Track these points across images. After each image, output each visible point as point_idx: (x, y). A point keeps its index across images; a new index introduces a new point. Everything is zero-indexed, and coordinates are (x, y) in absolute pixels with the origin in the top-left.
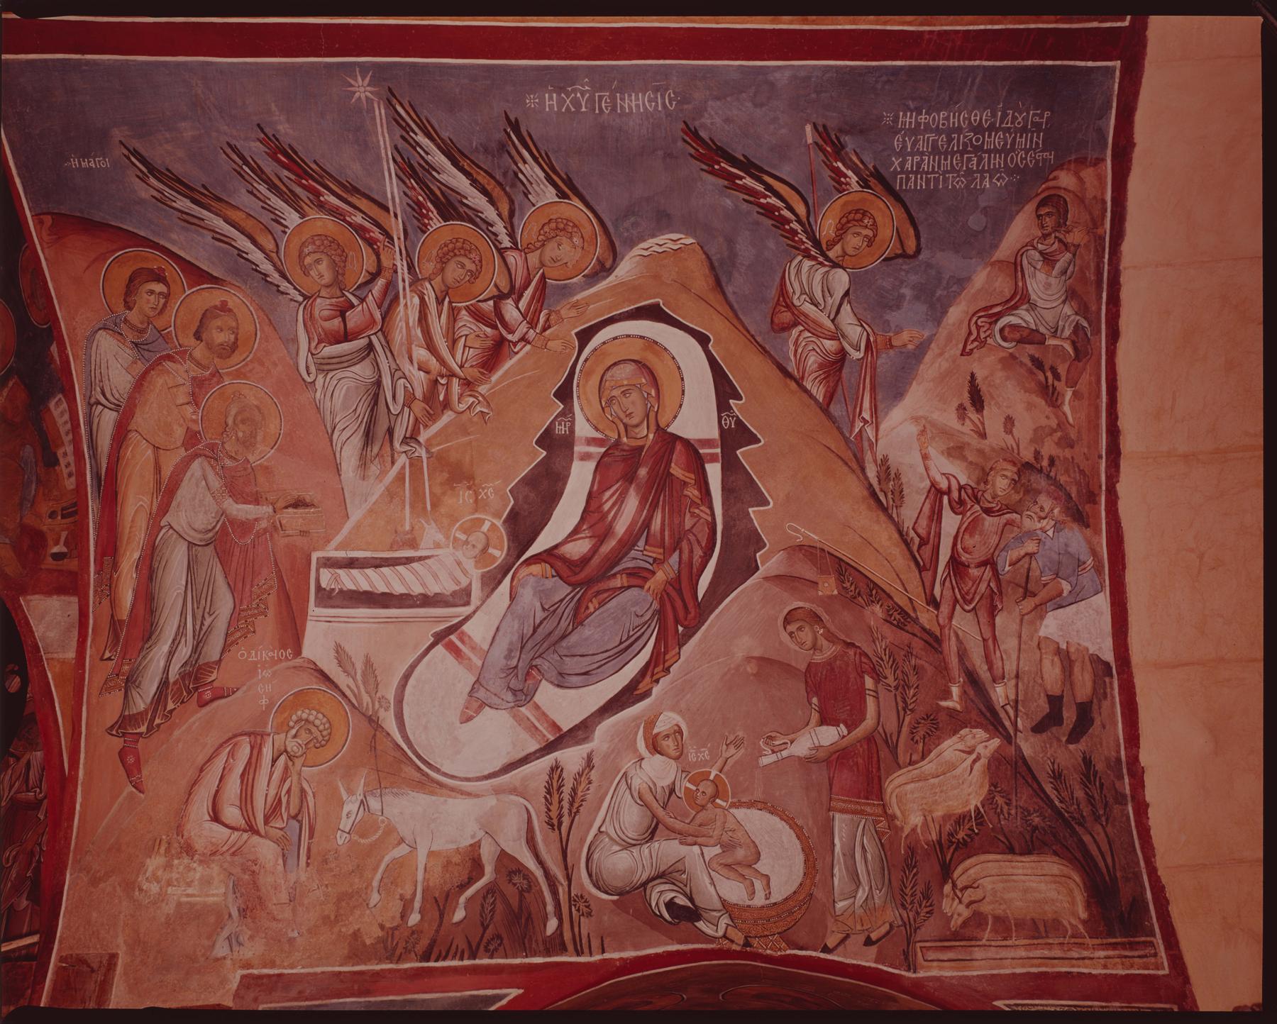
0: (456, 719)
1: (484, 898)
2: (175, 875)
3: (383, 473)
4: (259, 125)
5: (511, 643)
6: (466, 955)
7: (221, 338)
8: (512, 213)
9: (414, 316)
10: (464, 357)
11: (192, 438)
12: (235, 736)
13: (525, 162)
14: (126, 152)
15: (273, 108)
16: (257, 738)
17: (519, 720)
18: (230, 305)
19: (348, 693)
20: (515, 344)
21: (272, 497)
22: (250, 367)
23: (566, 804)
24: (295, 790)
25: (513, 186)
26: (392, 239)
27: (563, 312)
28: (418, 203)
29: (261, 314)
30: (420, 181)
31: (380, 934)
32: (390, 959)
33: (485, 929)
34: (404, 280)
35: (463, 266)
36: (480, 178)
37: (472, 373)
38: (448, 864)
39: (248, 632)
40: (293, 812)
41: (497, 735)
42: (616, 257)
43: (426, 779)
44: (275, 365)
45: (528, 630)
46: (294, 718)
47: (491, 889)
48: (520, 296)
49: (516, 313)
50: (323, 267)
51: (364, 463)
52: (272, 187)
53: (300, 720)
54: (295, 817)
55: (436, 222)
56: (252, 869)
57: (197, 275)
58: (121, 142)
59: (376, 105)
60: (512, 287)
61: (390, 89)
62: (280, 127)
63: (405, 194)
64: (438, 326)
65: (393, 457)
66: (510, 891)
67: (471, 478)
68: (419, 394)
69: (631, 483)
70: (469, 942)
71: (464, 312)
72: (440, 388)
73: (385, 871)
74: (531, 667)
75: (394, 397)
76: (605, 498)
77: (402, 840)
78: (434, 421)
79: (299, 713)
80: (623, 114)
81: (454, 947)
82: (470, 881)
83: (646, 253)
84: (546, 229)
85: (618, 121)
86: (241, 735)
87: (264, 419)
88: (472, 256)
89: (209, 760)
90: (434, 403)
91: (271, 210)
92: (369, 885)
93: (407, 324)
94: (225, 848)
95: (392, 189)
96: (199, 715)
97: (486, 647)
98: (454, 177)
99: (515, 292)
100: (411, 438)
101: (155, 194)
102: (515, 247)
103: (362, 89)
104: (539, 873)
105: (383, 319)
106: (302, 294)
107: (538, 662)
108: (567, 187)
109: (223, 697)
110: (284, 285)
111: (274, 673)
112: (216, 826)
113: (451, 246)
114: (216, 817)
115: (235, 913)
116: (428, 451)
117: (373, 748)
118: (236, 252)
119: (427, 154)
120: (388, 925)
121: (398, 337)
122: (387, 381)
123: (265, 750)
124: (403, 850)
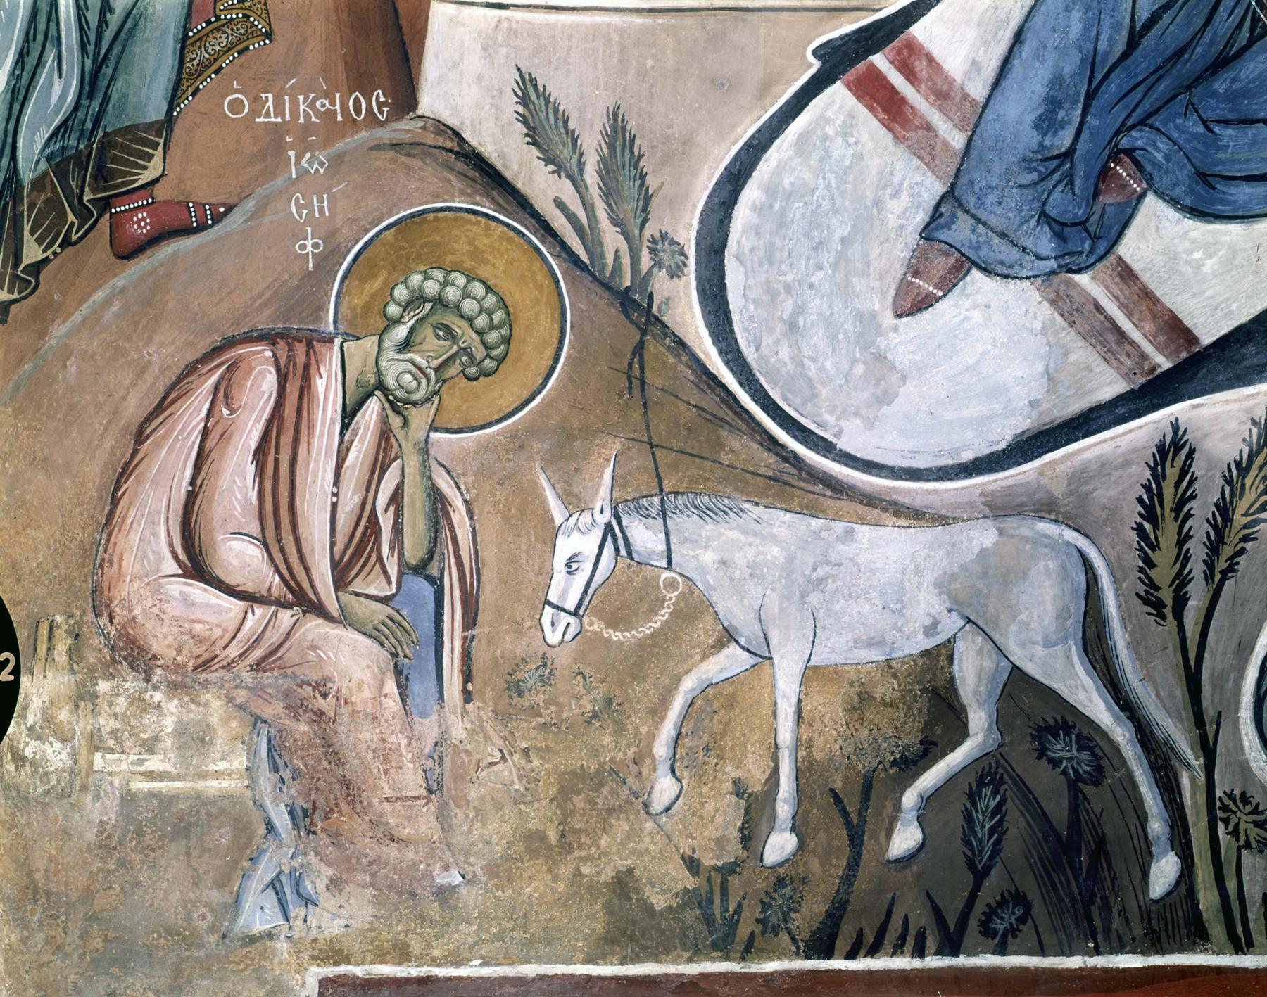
0: (881, 305)
1: (973, 796)
2: (106, 723)
5: (1057, 81)
6: (931, 943)
12: (230, 343)
16: (296, 347)
17: (1073, 310)
19: (559, 223)
23: (1197, 549)
24: (415, 496)
31: (690, 883)
32: (723, 947)
33: (980, 876)
38: (861, 702)
39: (251, 34)
40: (413, 554)
41: (998, 349)
43: (798, 473)
45: (1112, 42)
46: (401, 292)
47: (987, 774)
53: (418, 299)
54: (420, 569)
56: (312, 699)
66: (1047, 784)
70: (937, 911)
73: (685, 716)
74: (1115, 156)
77: (728, 636)
79: (416, 279)
81: (896, 922)
82: (929, 752)
86: (249, 339)
89: (160, 408)
92: (643, 756)
94: (233, 651)
96: (119, 281)
97: (978, 91)
104: (1122, 734)
107: (1138, 138)
109: (187, 231)
111: (337, 162)
112: (199, 591)
114: (197, 566)
115: (282, 821)
117: (636, 382)
120: (709, 861)
123: (320, 384)
124: (731, 661)
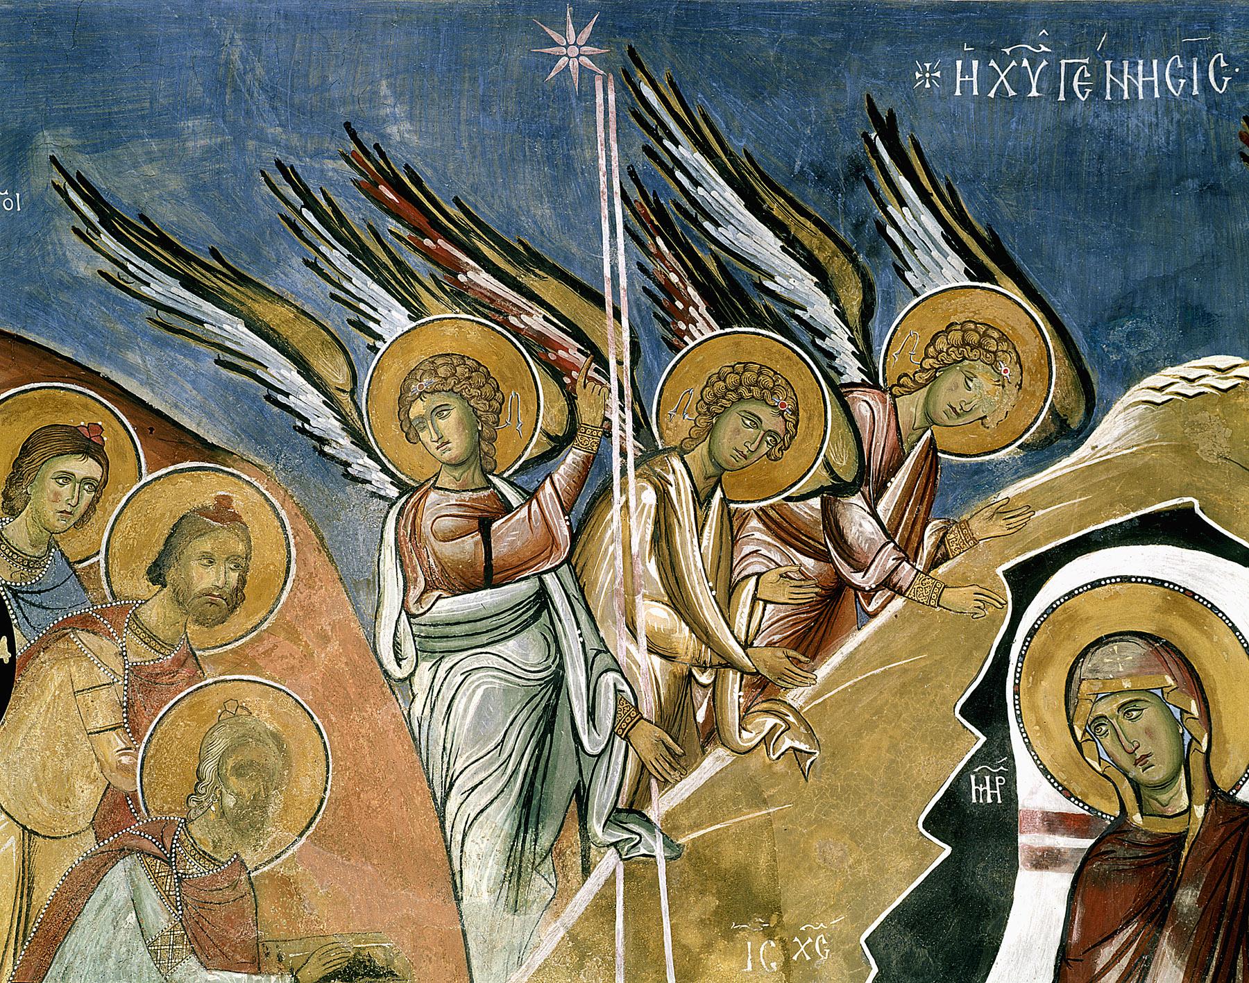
3: (562, 895)
4: (347, 126)
7: (206, 578)
8: (867, 311)
9: (642, 531)
10: (753, 621)
11: (116, 810)
13: (902, 203)
14: (60, 180)
15: (384, 89)
18: (238, 505)
20: (869, 598)
21: (292, 954)
22: (267, 644)
25: (873, 252)
26: (605, 364)
27: (975, 525)
28: (668, 288)
29: (303, 525)
30: (676, 242)
34: (623, 454)
35: (756, 422)
36: (802, 236)
37: (769, 659)
42: (1093, 410)
44: (325, 639)
48: (881, 489)
49: (870, 526)
50: (450, 425)
51: (516, 871)
52: (360, 254)
55: (703, 327)
57: (172, 440)
58: (53, 160)
59: (599, 84)
60: (863, 469)
61: (632, 52)
62: (392, 130)
63: (641, 267)
64: (695, 553)
65: (585, 857)
67: (772, 908)
68: (648, 706)
69: (1161, 926)
71: (754, 522)
72: (698, 693)
75: (591, 713)
76: (1101, 962)
78: (685, 771)
80: (1118, 102)
83: (1159, 398)
84: (941, 344)
85: (1105, 116)
87: (288, 764)
88: (776, 400)
90: (685, 728)
91: (350, 302)
93: (627, 548)
95: (615, 258)
98: (749, 234)
99: (867, 480)
100: (631, 810)
101: (108, 267)
102: (871, 380)
103: (574, 51)
105: (574, 538)
106: (397, 483)
108: (989, 256)
110: (361, 463)
113: (732, 379)
116: (668, 843)
118: (264, 391)
119: (696, 184)
121: (606, 576)
122: (576, 677)
